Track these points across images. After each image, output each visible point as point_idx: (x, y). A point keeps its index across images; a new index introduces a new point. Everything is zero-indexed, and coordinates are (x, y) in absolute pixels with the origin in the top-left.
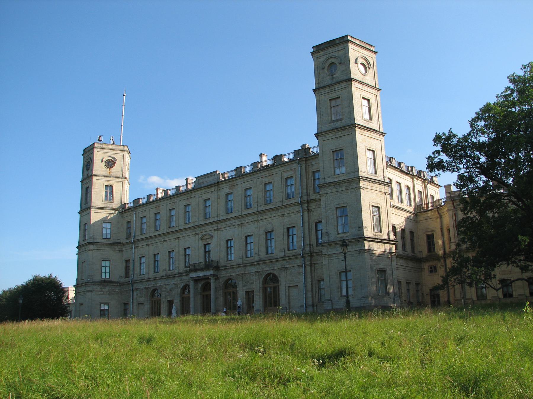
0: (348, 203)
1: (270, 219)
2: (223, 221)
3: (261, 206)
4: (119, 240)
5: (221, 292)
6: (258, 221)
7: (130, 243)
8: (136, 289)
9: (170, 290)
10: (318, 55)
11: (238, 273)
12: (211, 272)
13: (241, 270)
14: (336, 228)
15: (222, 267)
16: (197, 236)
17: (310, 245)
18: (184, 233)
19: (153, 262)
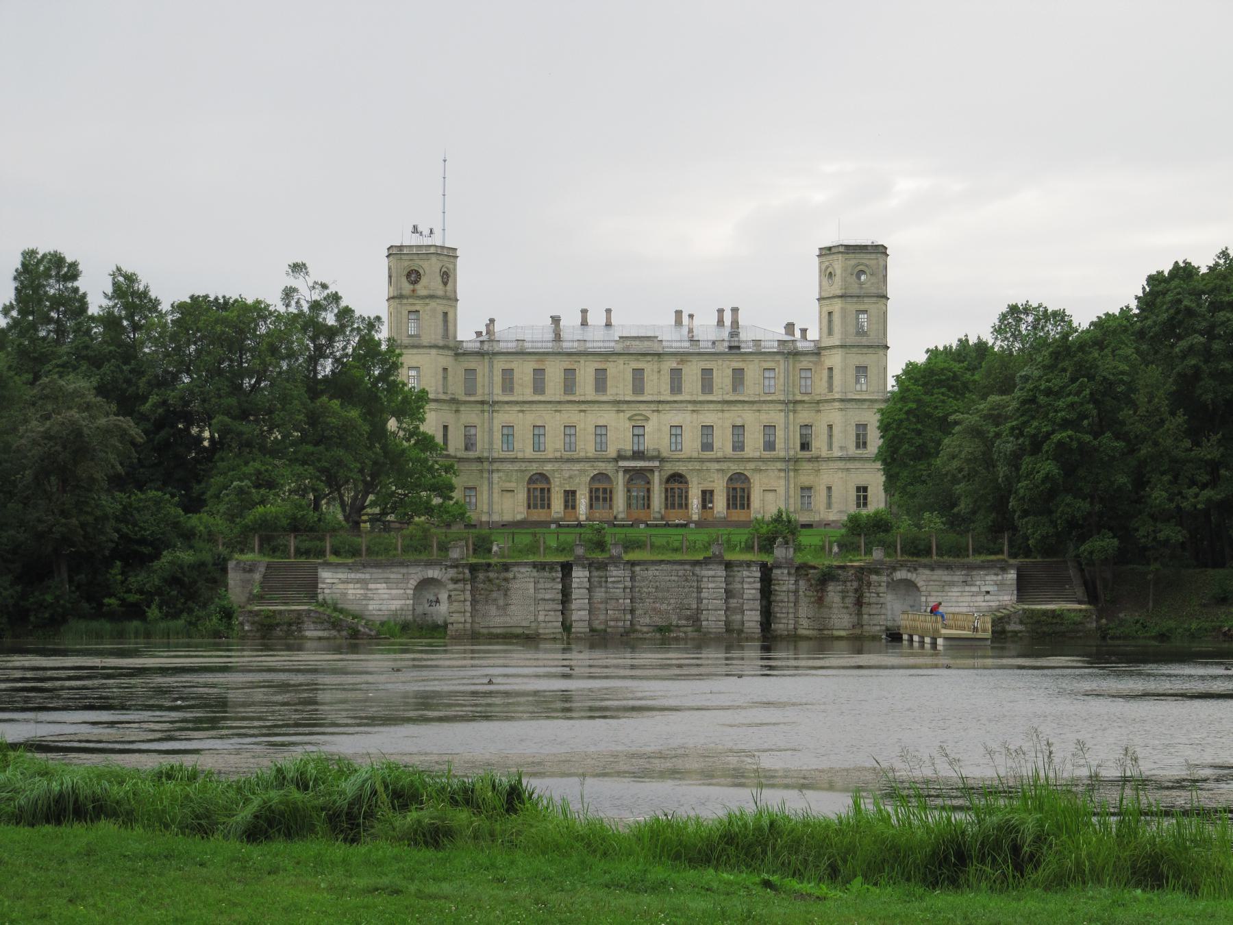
9: (570, 477)
12: (657, 464)
13: (697, 466)
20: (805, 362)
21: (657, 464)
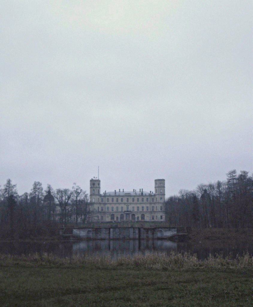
12: (130, 213)
13: (136, 213)
20: (153, 197)
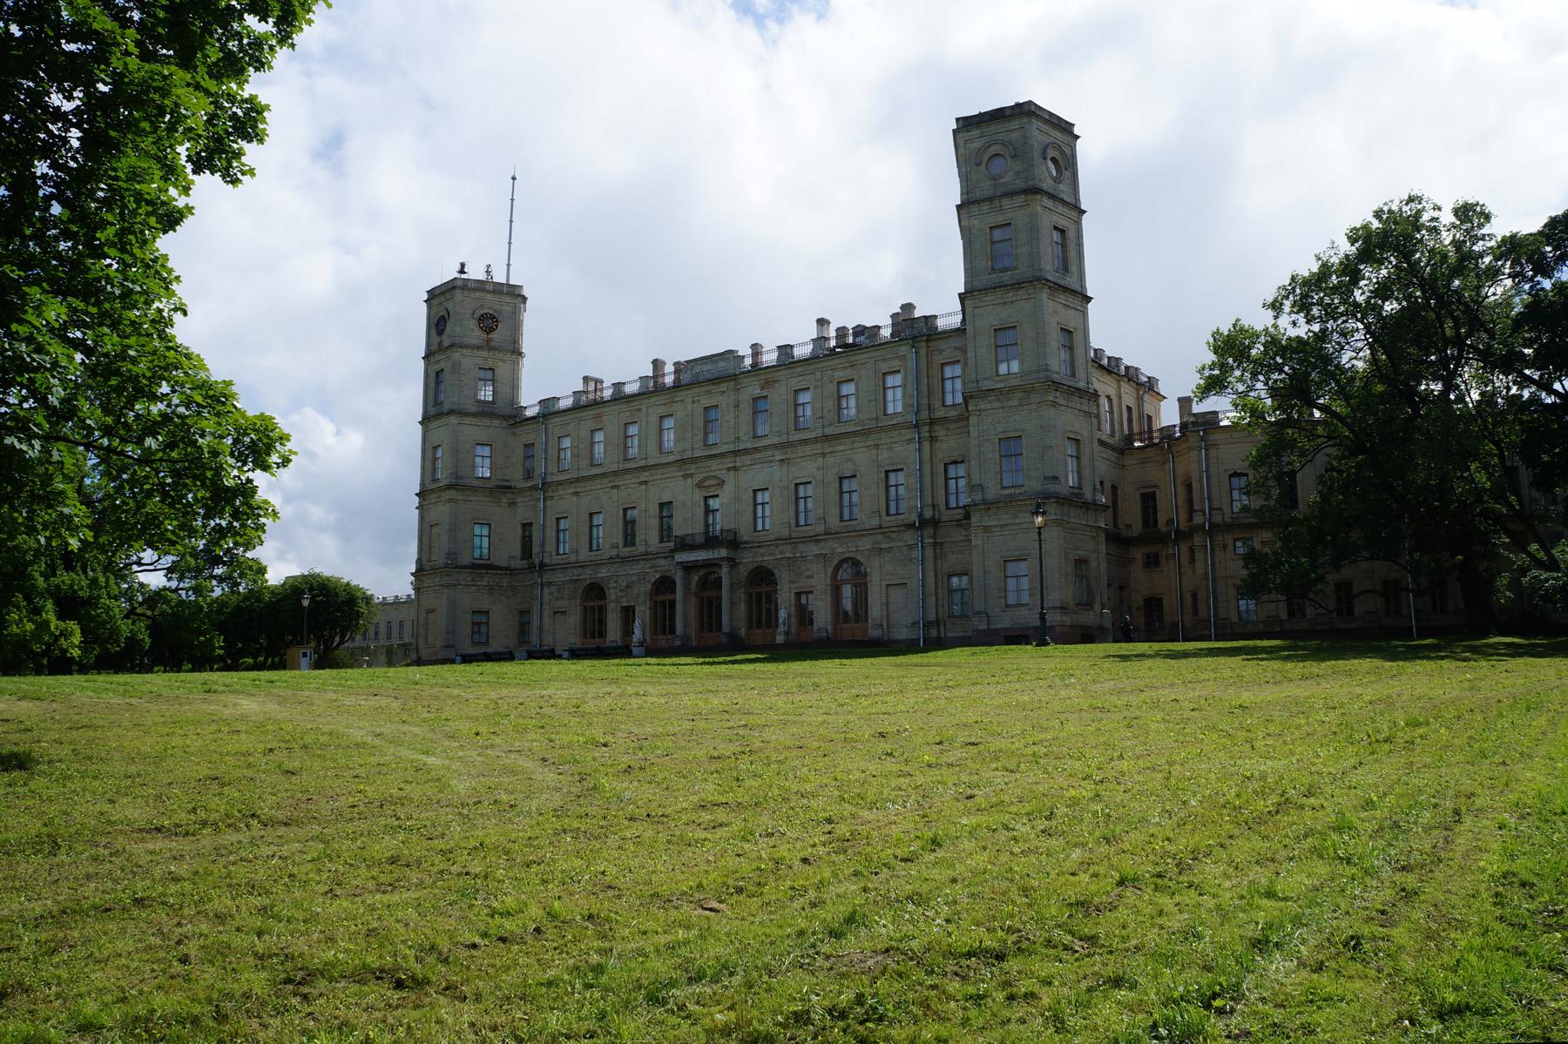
0: (1024, 431)
1: (849, 452)
2: (747, 451)
3: (830, 425)
4: (506, 481)
5: (741, 593)
6: (824, 455)
7: (534, 488)
8: (550, 584)
9: (628, 587)
10: (967, 135)
11: (779, 556)
12: (723, 553)
14: (999, 476)
15: (747, 542)
16: (689, 480)
17: (933, 506)
18: (659, 471)
19: (586, 529)
21: (723, 553)
